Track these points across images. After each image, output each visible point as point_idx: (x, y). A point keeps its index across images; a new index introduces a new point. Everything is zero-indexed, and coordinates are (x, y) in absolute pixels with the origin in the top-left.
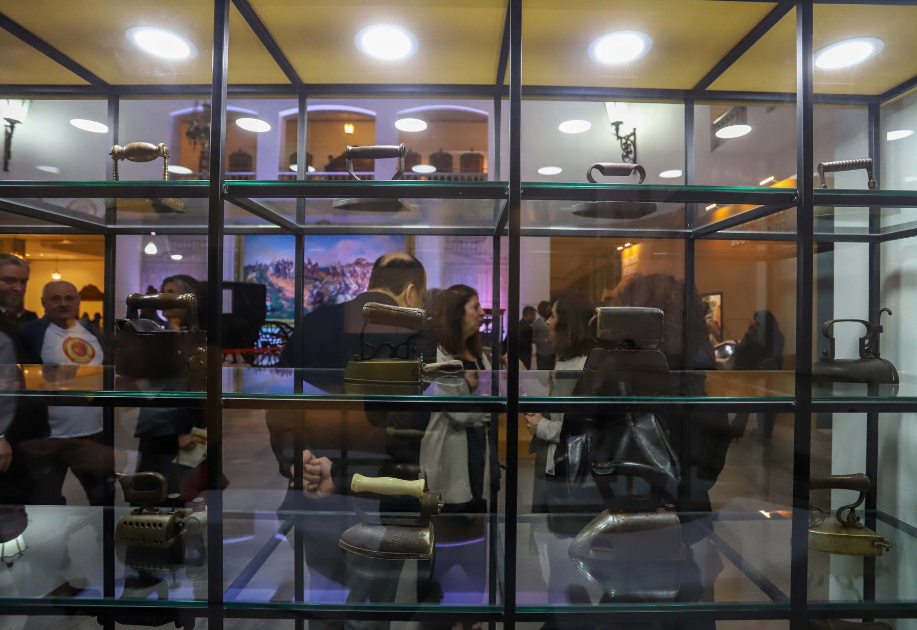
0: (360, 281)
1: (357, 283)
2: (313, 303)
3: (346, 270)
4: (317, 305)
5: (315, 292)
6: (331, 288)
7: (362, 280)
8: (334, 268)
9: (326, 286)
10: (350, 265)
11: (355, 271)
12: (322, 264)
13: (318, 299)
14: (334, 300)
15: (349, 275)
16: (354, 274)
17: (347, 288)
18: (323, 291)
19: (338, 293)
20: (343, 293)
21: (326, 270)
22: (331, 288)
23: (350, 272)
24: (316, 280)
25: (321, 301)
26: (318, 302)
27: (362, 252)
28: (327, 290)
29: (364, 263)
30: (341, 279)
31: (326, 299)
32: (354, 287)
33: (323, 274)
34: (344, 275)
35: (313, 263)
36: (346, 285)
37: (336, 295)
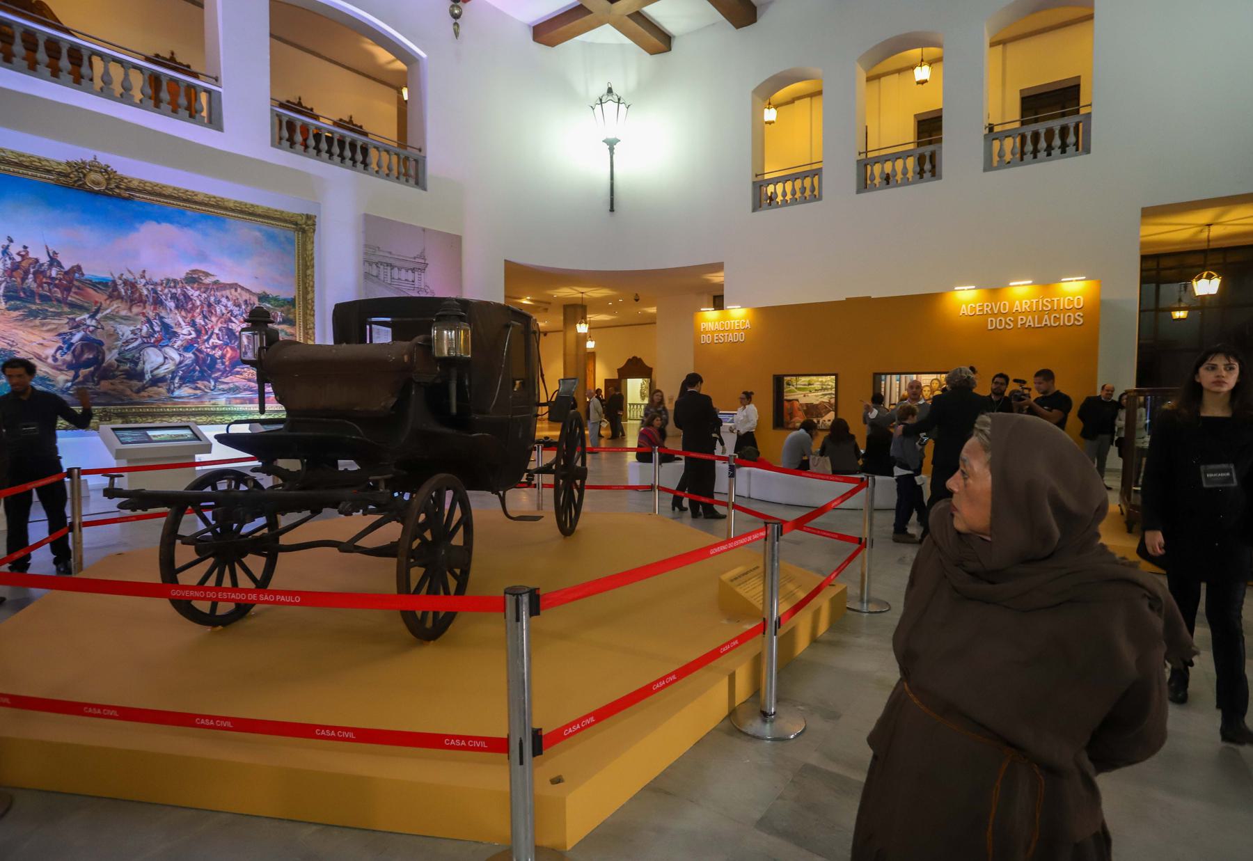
0: (199, 321)
1: (193, 324)
2: (74, 366)
3: (164, 293)
4: (84, 372)
5: (77, 338)
6: (126, 330)
7: (205, 317)
8: (132, 285)
9: (108, 325)
10: (170, 282)
11: (188, 298)
12: (95, 270)
13: (88, 356)
14: (135, 361)
15: (171, 304)
16: (183, 303)
17: (169, 333)
18: (99, 336)
19: (145, 344)
20: (157, 345)
21: (109, 288)
22: (126, 330)
23: (174, 297)
24: (82, 308)
25: (97, 361)
26: (87, 364)
27: (203, 257)
28: (114, 335)
29: (208, 281)
30: (151, 314)
31: (111, 357)
32: (186, 332)
33: (100, 297)
34: (158, 302)
35: (67, 266)
36: (166, 327)
37: (140, 348)
